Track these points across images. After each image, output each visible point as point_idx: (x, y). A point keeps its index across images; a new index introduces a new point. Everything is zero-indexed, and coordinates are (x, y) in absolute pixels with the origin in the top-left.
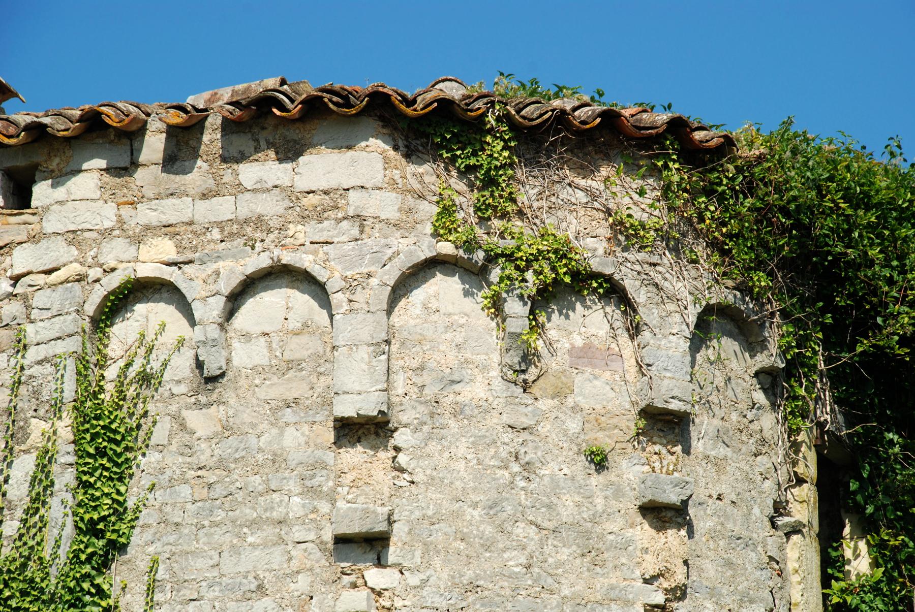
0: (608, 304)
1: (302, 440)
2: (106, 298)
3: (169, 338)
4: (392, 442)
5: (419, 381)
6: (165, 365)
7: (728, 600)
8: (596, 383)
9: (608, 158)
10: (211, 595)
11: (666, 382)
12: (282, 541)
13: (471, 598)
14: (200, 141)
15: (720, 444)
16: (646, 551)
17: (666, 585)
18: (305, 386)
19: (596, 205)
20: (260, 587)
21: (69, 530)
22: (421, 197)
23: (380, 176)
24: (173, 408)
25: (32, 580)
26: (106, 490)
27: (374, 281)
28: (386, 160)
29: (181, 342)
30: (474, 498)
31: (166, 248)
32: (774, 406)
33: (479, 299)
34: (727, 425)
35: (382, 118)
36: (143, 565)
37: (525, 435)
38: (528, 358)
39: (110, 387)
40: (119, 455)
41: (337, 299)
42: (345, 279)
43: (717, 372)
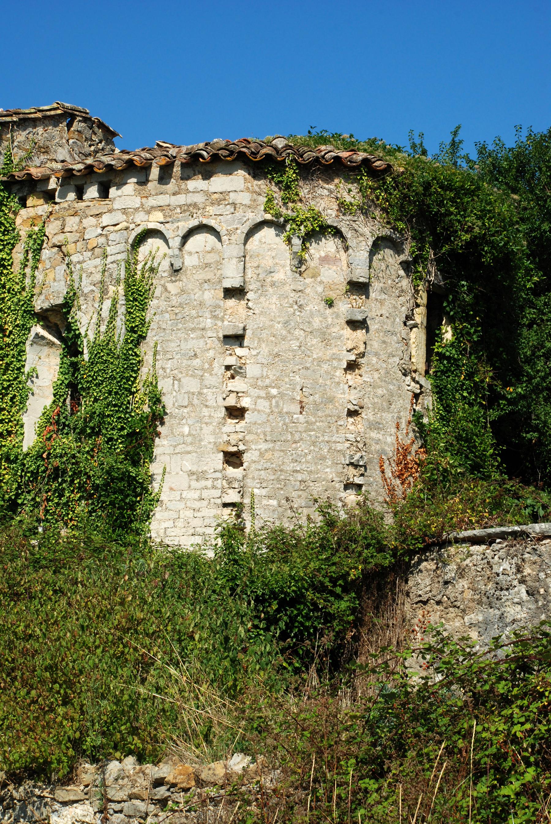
0: (335, 238)
1: (211, 296)
2: (136, 236)
3: (160, 254)
4: (246, 297)
5: (257, 272)
6: (159, 264)
7: (383, 356)
8: (330, 271)
9: (338, 176)
10: (177, 357)
11: (358, 270)
12: (203, 337)
13: (277, 359)
14: (172, 171)
15: (383, 294)
16: (348, 339)
17: (356, 352)
18: (213, 274)
19: (332, 196)
20: (195, 355)
21: (124, 330)
22: (260, 194)
23: (242, 186)
24: (162, 282)
25: (111, 349)
26: (138, 315)
27: (239, 231)
28: (245, 179)
29: (165, 255)
30: (279, 320)
31: (158, 216)
32: (408, 276)
33: (282, 237)
34: (386, 285)
35: (244, 162)
36: (152, 344)
37: (300, 294)
38: (301, 262)
39: (139, 273)
40: (142, 301)
41: (224, 238)
42: (227, 230)
43: (382, 264)
